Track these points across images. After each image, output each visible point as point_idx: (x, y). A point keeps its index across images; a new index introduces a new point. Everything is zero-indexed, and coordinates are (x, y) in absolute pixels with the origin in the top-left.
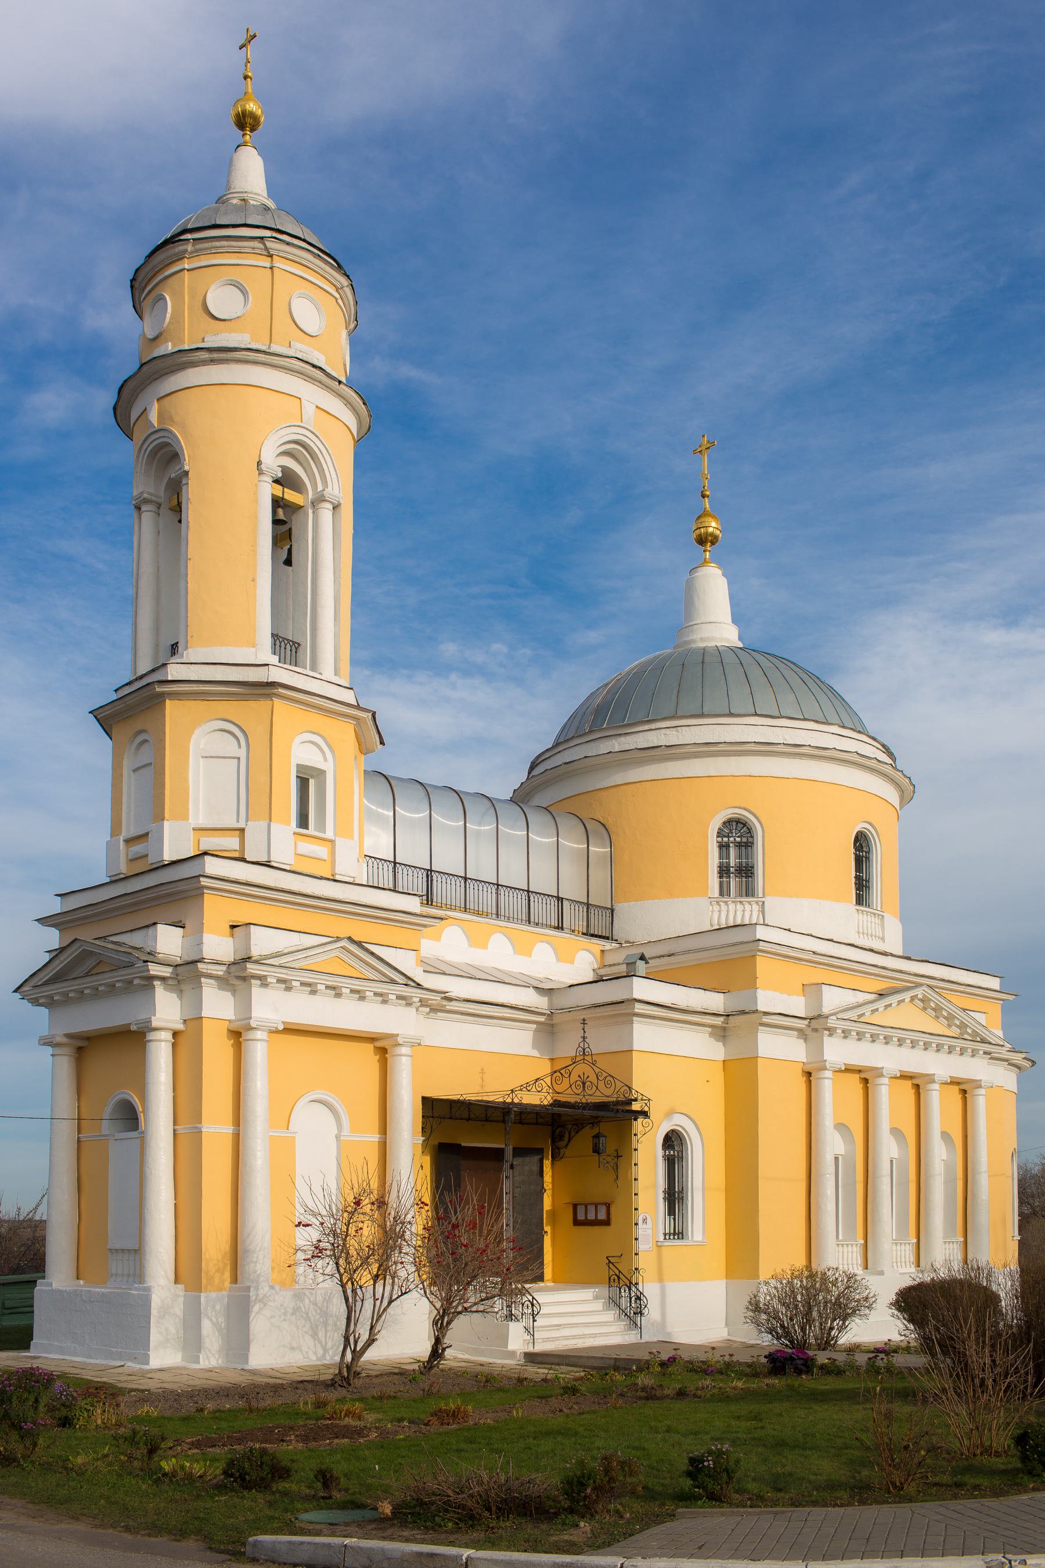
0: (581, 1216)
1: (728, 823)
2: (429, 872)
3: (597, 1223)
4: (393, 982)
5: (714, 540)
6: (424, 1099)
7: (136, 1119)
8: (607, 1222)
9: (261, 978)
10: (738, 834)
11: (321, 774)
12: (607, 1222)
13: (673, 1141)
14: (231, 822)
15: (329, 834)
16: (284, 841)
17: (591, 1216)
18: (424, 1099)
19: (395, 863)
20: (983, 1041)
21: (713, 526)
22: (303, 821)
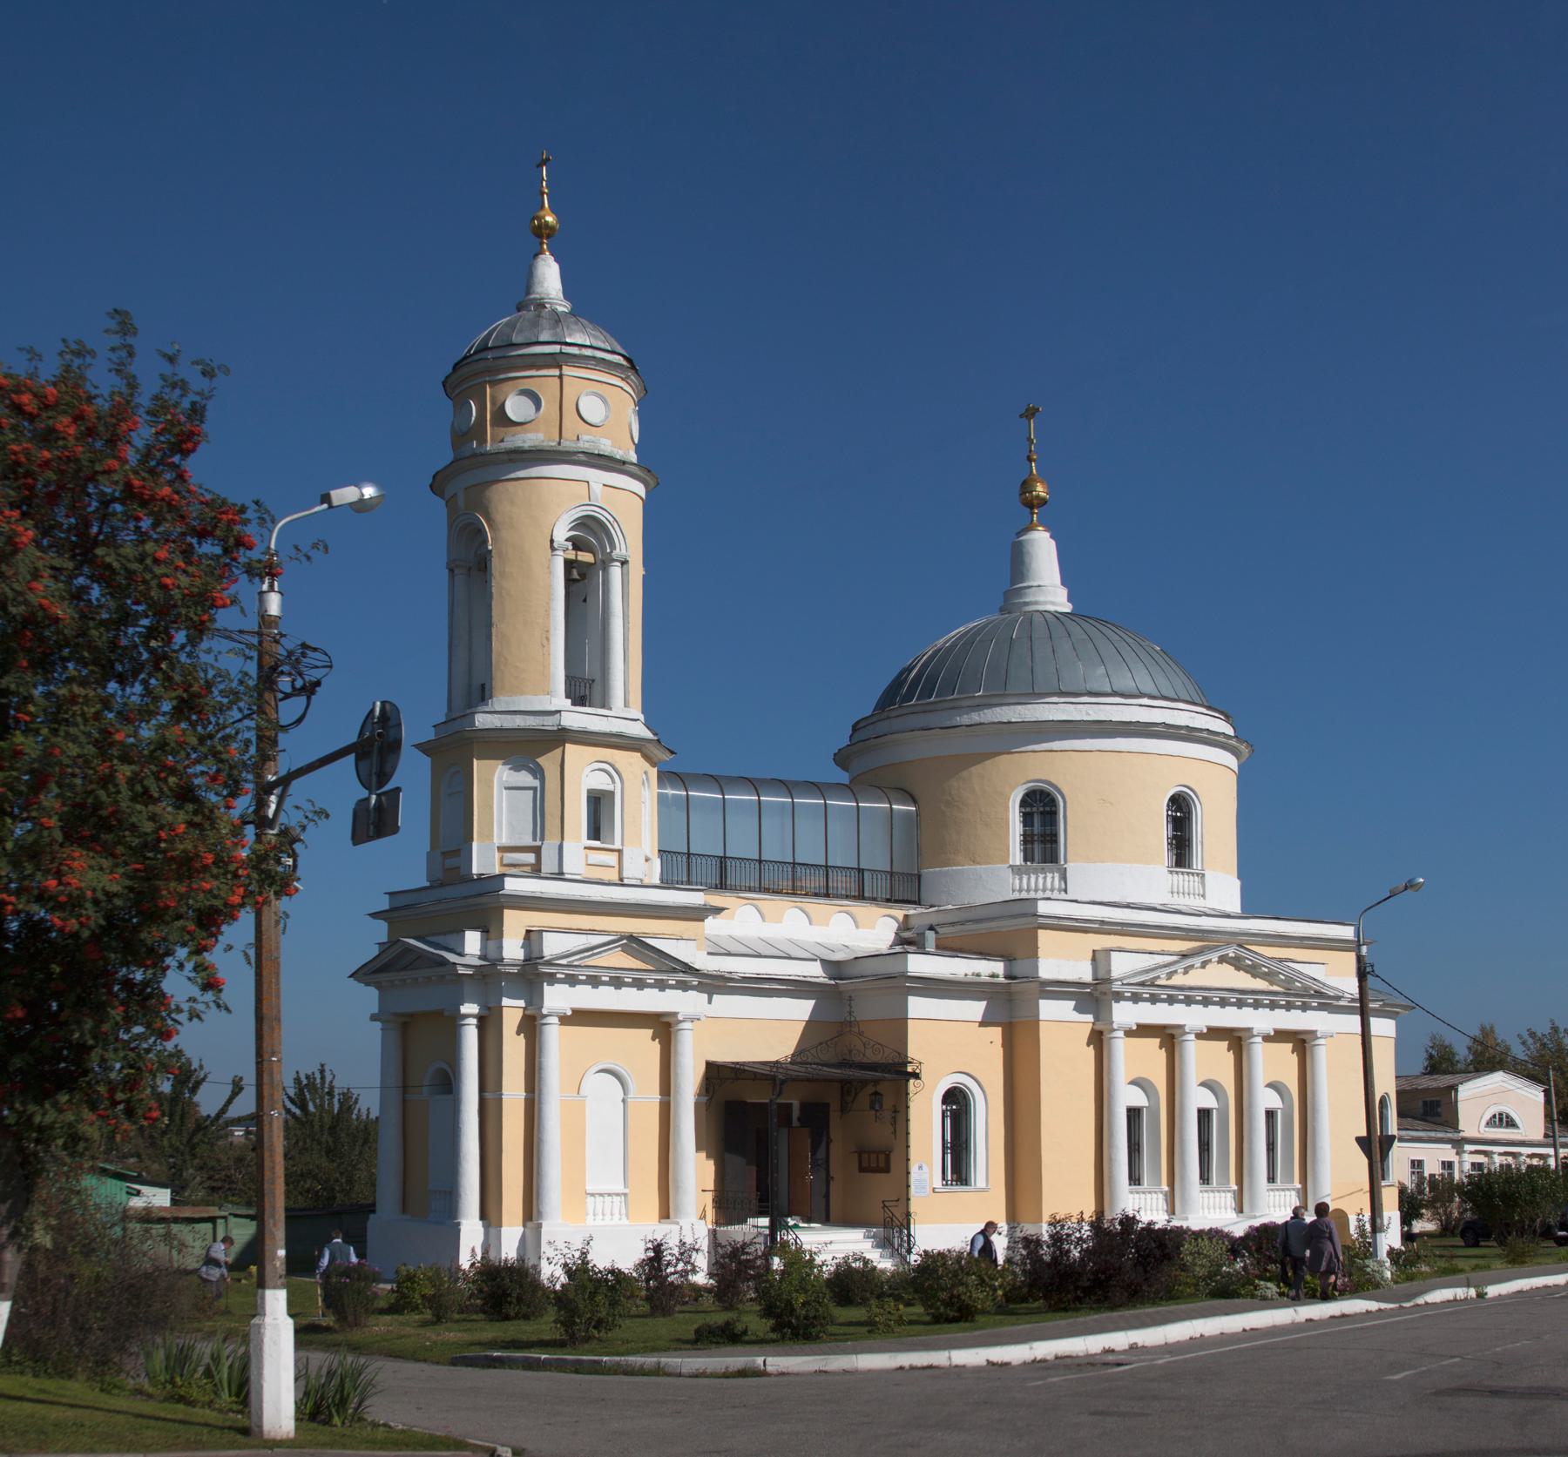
0: (865, 1164)
1: (1023, 803)
2: (723, 860)
3: (877, 1170)
4: (674, 970)
5: (1043, 502)
6: (709, 1065)
7: (450, 1084)
8: (887, 1170)
9: (553, 975)
10: (1042, 810)
11: (610, 795)
12: (887, 1170)
13: (956, 1100)
14: (528, 841)
15: (617, 845)
16: (577, 852)
17: (874, 1165)
18: (709, 1065)
19: (689, 854)
20: (1318, 994)
21: (1040, 490)
22: (595, 832)
